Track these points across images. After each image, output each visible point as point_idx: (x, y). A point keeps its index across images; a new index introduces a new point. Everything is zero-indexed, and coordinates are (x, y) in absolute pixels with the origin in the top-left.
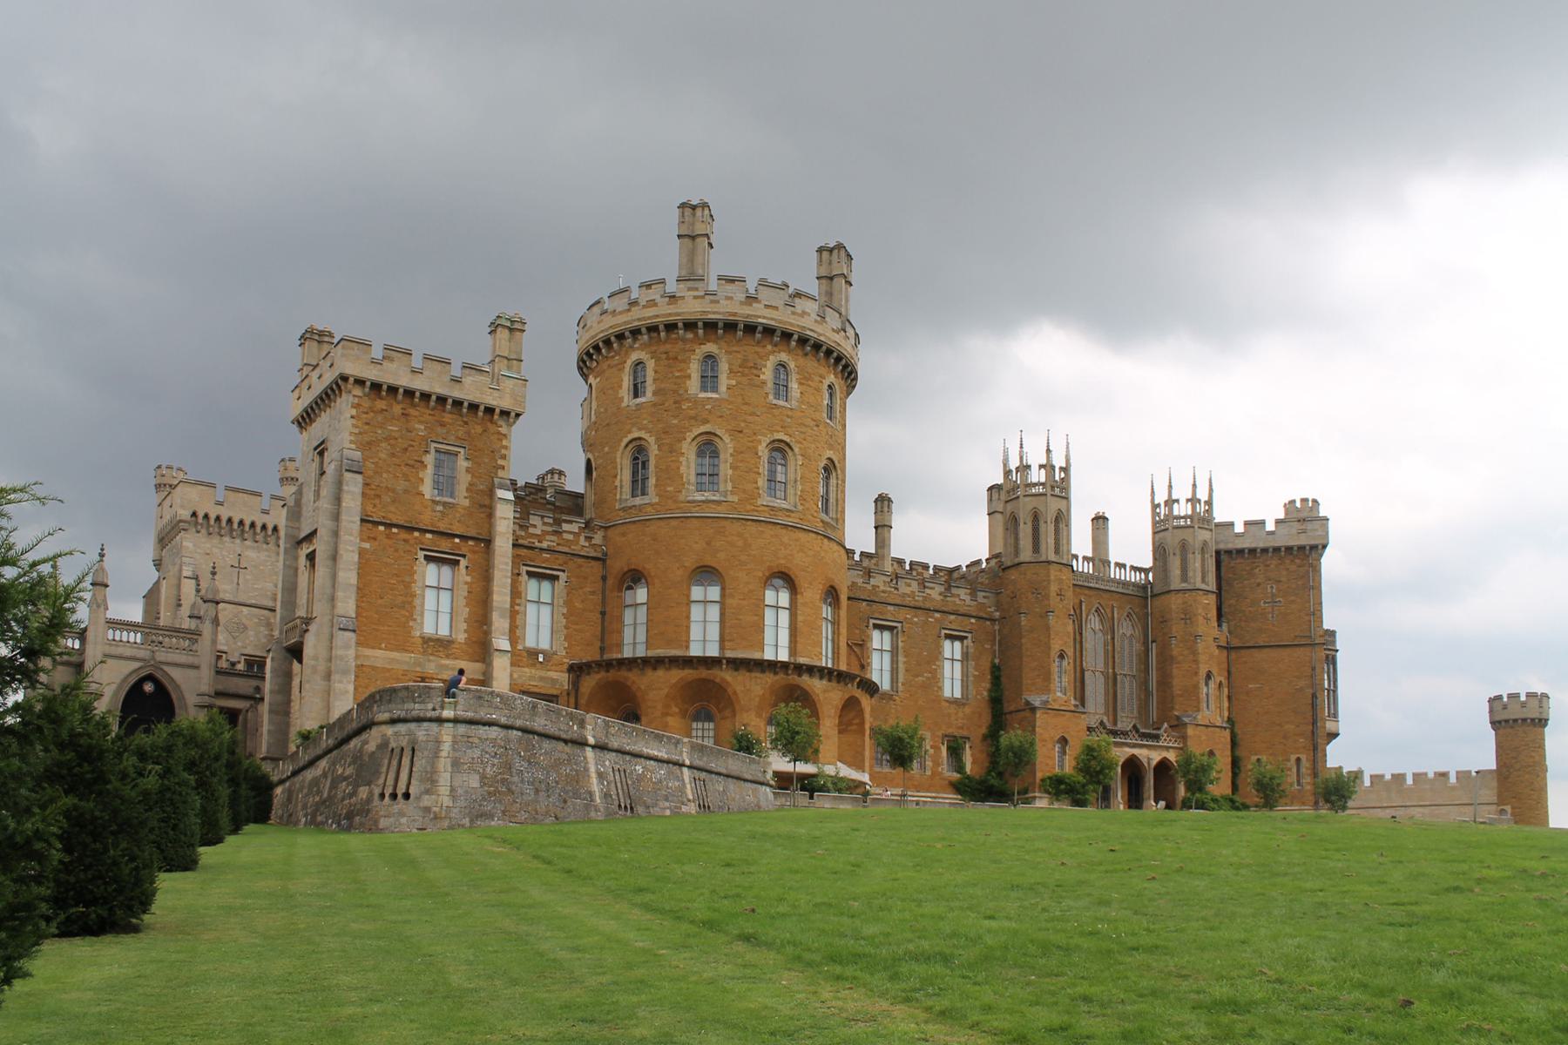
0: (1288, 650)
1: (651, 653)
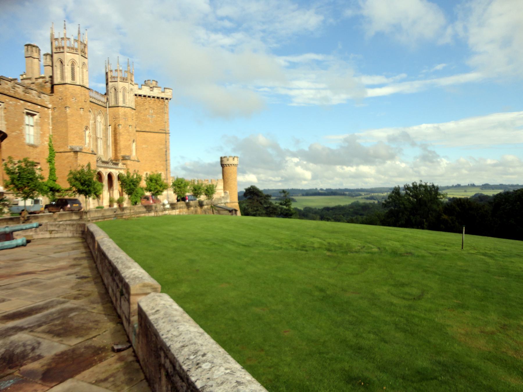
0: (157, 134)
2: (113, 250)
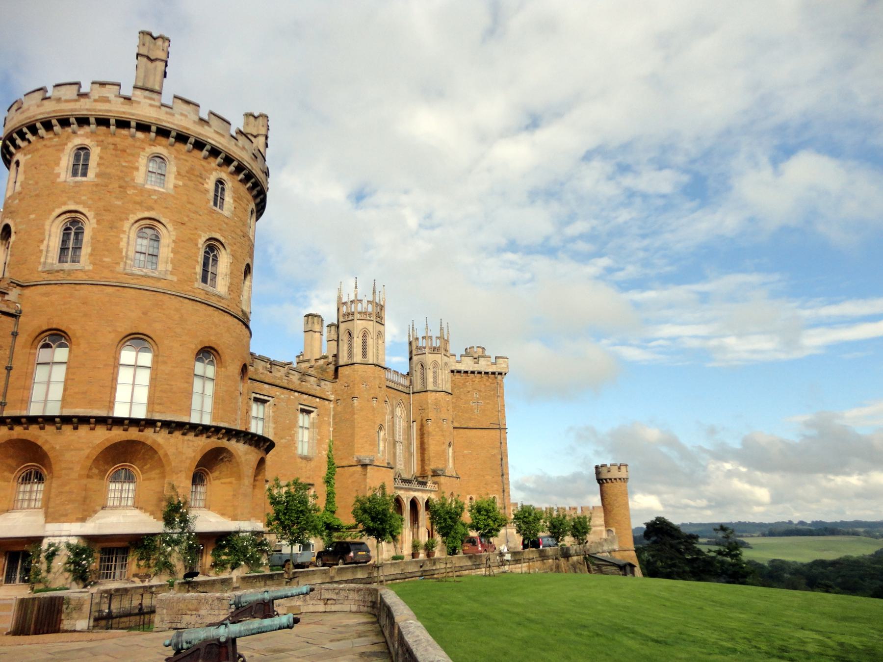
1: (67, 412)
2: (424, 644)
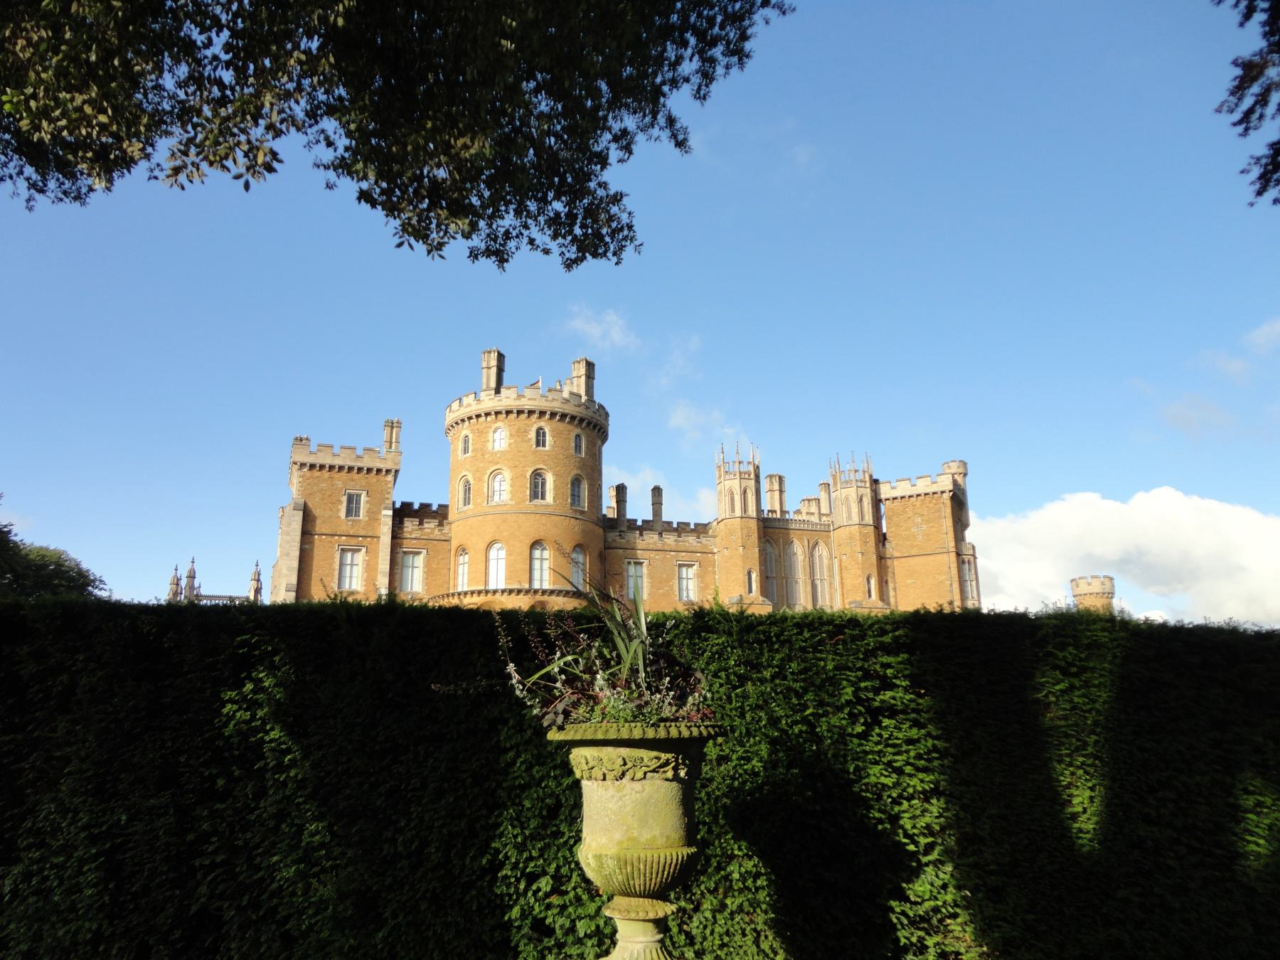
0: (932, 557)
